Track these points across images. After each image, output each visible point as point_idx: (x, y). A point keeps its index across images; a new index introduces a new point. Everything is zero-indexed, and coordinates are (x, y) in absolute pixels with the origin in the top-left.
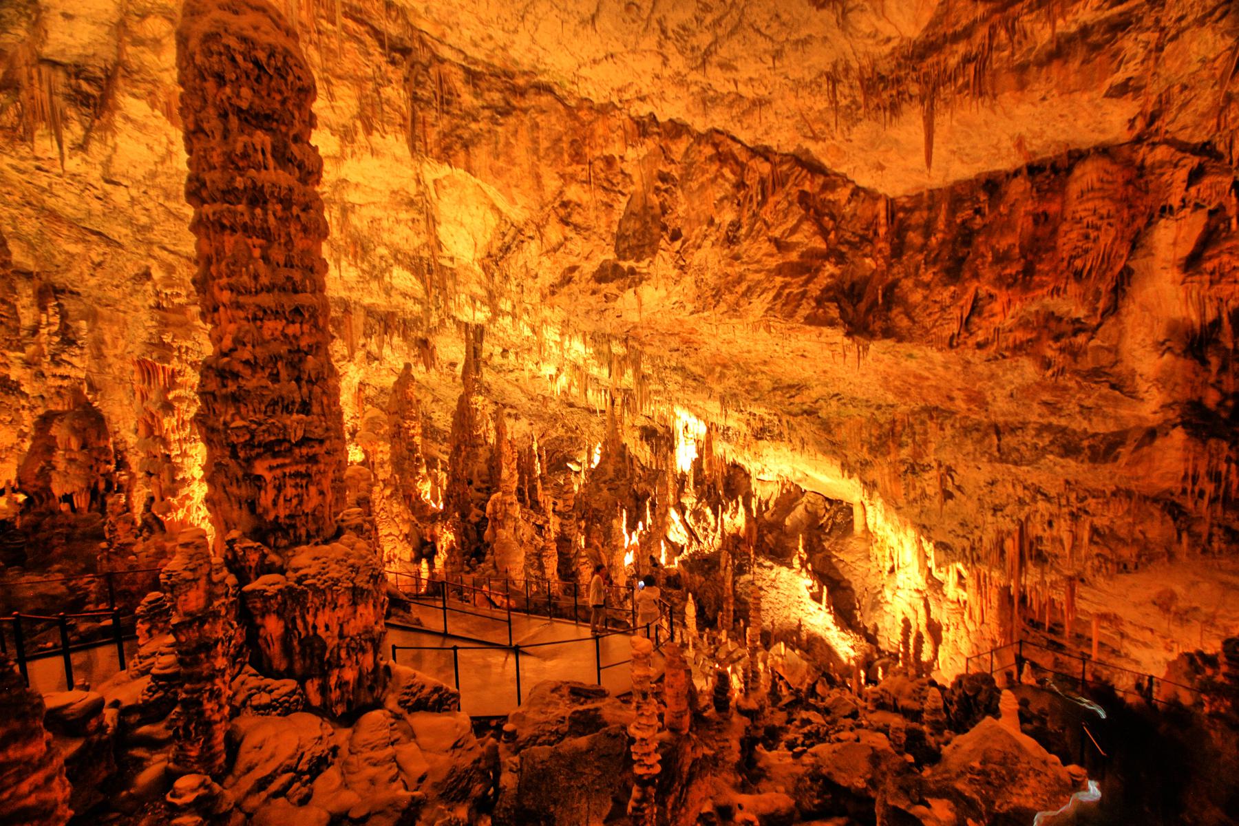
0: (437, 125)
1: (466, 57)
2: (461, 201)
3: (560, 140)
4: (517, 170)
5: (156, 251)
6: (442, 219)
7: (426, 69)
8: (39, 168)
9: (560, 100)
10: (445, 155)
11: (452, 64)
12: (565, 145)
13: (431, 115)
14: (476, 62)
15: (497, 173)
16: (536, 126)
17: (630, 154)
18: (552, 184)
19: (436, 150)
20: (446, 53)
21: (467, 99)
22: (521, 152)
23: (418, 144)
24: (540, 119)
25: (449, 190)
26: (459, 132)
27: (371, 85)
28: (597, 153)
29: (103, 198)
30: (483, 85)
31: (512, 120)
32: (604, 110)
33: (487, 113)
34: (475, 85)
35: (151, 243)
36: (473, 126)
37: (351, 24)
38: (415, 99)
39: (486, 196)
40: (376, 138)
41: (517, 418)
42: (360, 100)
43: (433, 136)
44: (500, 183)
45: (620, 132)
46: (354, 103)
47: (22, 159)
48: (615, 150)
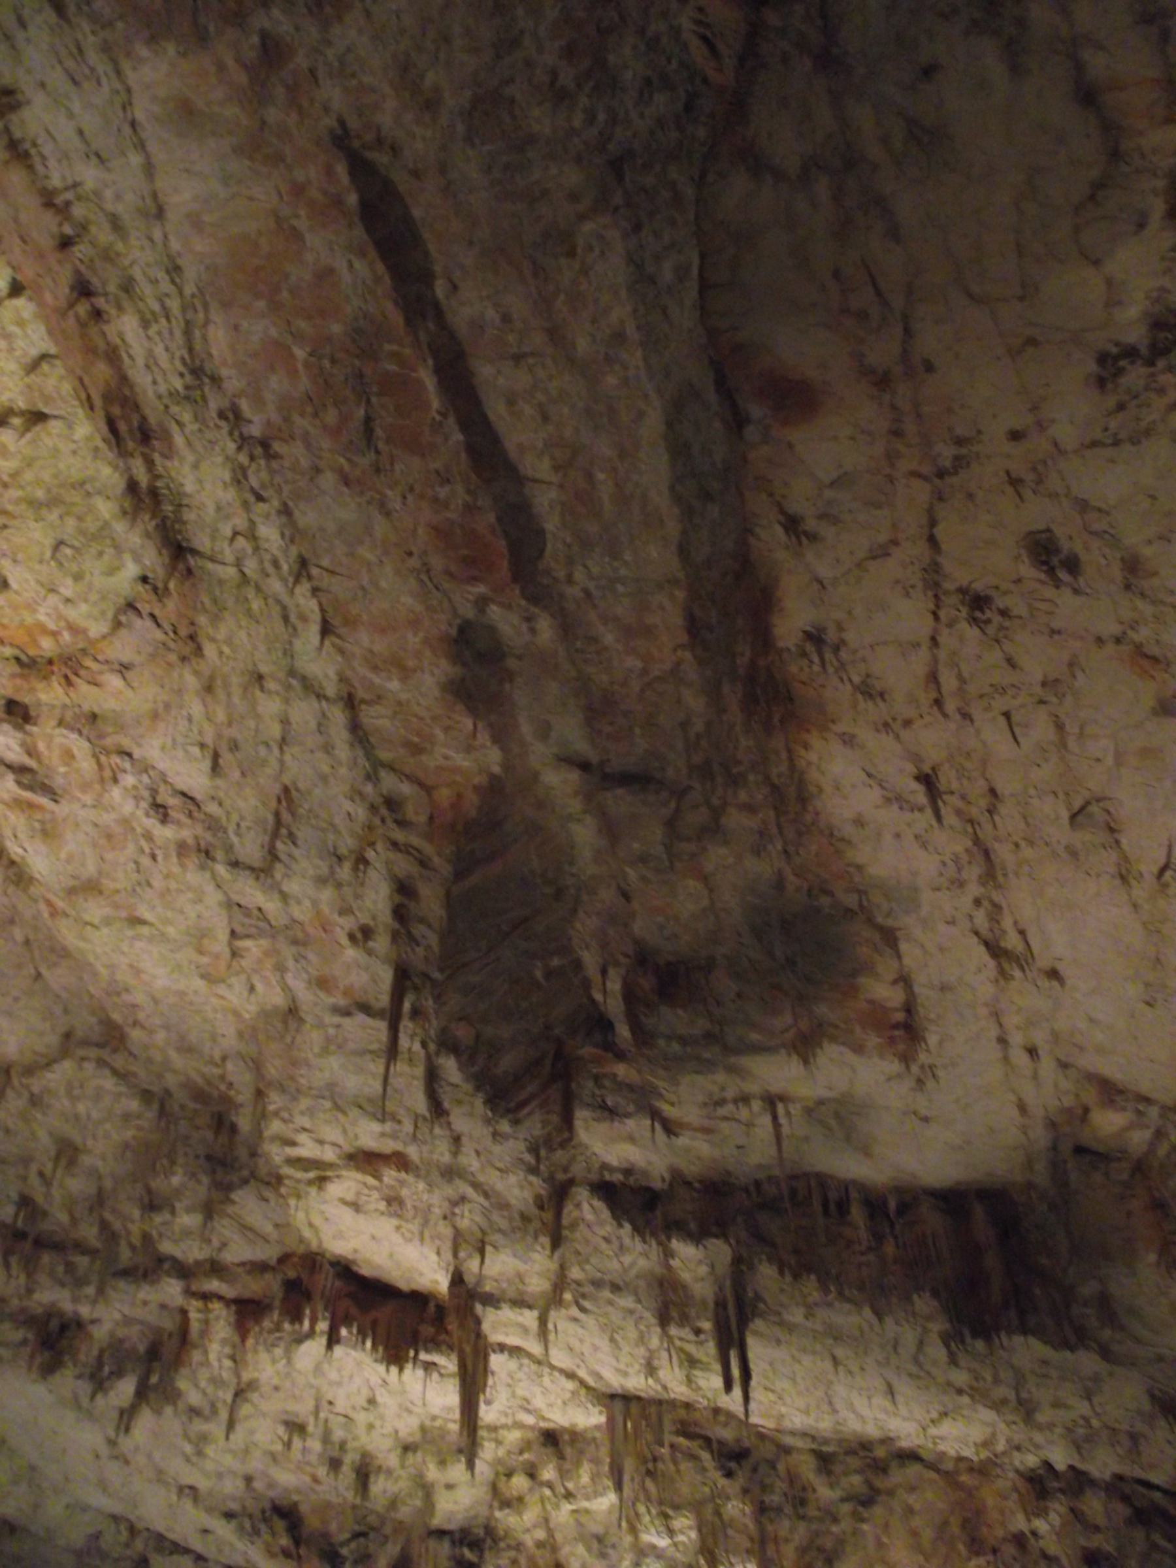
1: (813, 1438)
7: (773, 1465)
9: (931, 1466)
11: (799, 1450)
12: (955, 1529)
13: (784, 1526)
14: (826, 1442)
16: (910, 1511)
20: (789, 1440)
21: (825, 1493)
24: (911, 1499)
28: (1000, 1533)
31: (878, 1511)
32: (982, 1470)
33: (846, 1508)
34: (829, 1473)
36: (835, 1529)
37: (681, 1440)
38: (762, 1509)
42: (700, 1531)
45: (1015, 1496)
46: (693, 1535)
48: (1019, 1523)
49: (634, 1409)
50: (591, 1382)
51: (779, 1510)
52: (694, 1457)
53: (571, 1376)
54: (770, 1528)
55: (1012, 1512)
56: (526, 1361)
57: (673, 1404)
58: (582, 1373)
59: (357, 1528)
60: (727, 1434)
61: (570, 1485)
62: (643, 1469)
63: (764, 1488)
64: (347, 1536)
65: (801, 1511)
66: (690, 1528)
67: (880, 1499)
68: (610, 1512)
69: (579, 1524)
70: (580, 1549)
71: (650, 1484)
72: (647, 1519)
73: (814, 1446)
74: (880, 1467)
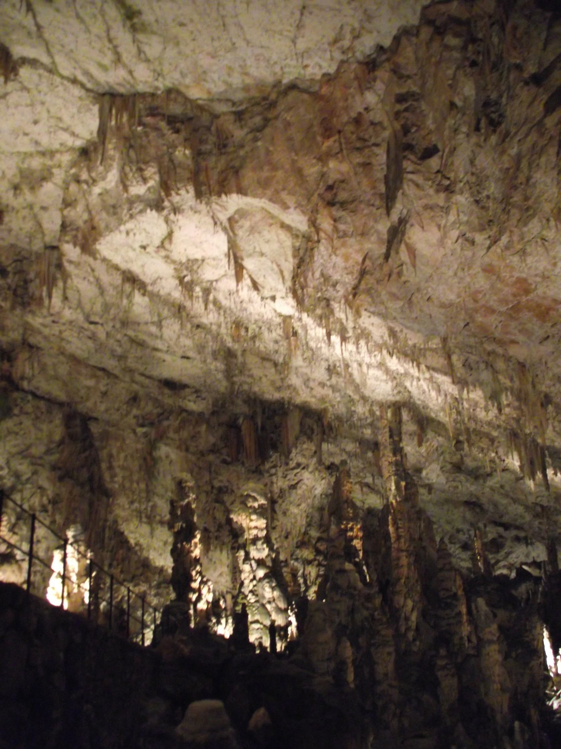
0: (215, 164)
2: (252, 230)
3: (311, 126)
4: (280, 174)
5: (138, 378)
6: (244, 254)
7: (209, 129)
8: (54, 322)
10: (223, 189)
11: (224, 114)
15: (264, 184)
16: (288, 125)
17: (371, 98)
18: (312, 170)
19: (216, 188)
21: (239, 134)
22: (281, 156)
23: (204, 188)
25: (240, 223)
26: (231, 164)
27: (166, 158)
28: (345, 118)
29: (93, 337)
30: (247, 116)
31: (267, 131)
35: (131, 371)
39: (273, 217)
40: (176, 199)
41: (527, 541)
43: (214, 176)
44: (269, 192)
47: (45, 317)
49: (118, 101)
50: (89, 85)
51: (210, 153)
52: (157, 129)
53: (74, 81)
54: (203, 164)
55: (353, 97)
56: (41, 71)
57: (143, 95)
58: (81, 78)
59: (16, 258)
60: (176, 109)
61: (94, 175)
62: (128, 145)
63: (201, 142)
64: (10, 261)
65: (223, 151)
66: (155, 173)
67: (270, 123)
68: (117, 187)
69: (103, 201)
70: (104, 215)
71: (132, 153)
72: (131, 175)
73: (234, 109)
74: (273, 105)
